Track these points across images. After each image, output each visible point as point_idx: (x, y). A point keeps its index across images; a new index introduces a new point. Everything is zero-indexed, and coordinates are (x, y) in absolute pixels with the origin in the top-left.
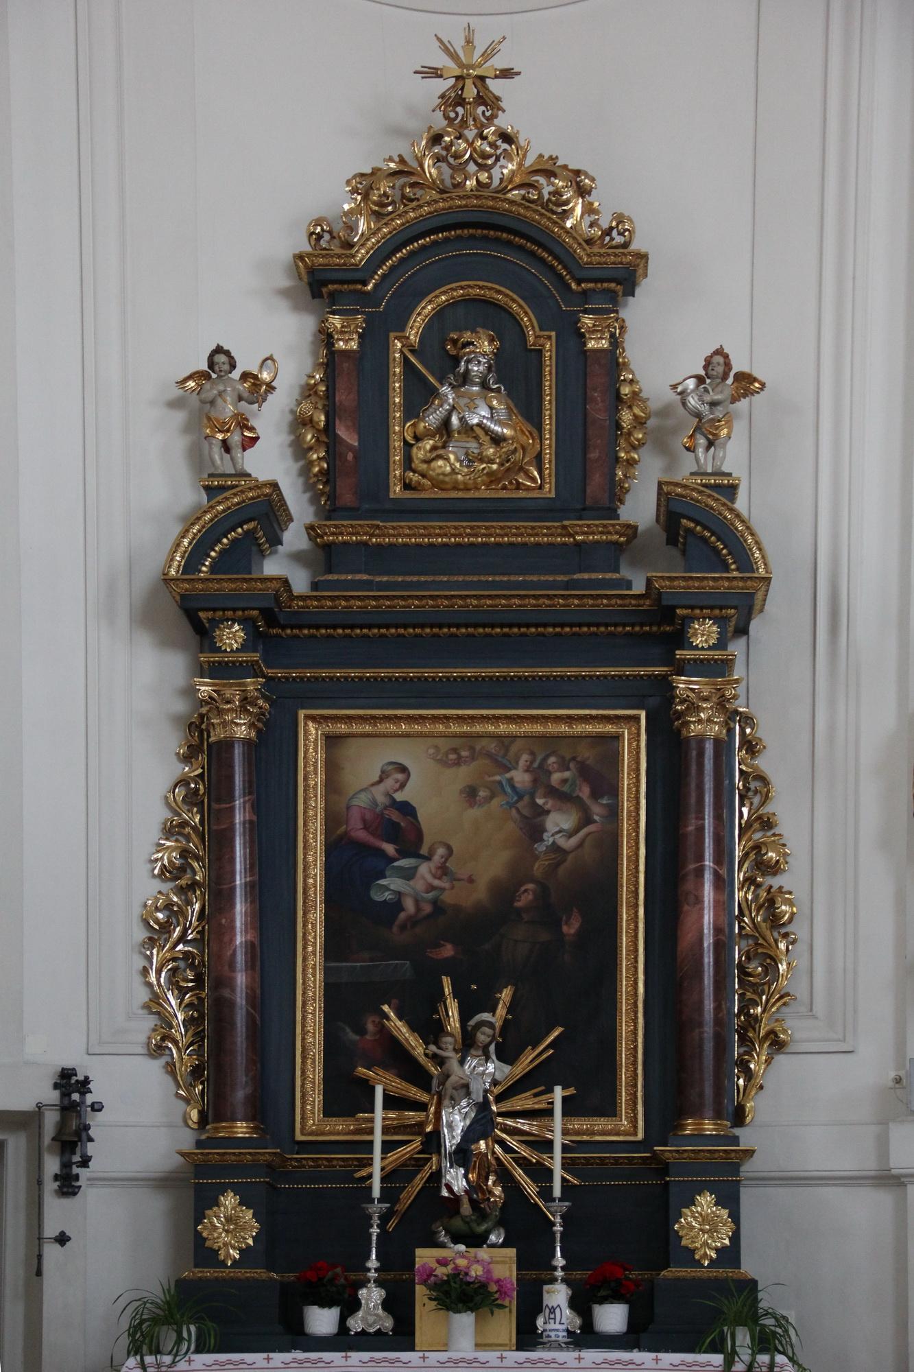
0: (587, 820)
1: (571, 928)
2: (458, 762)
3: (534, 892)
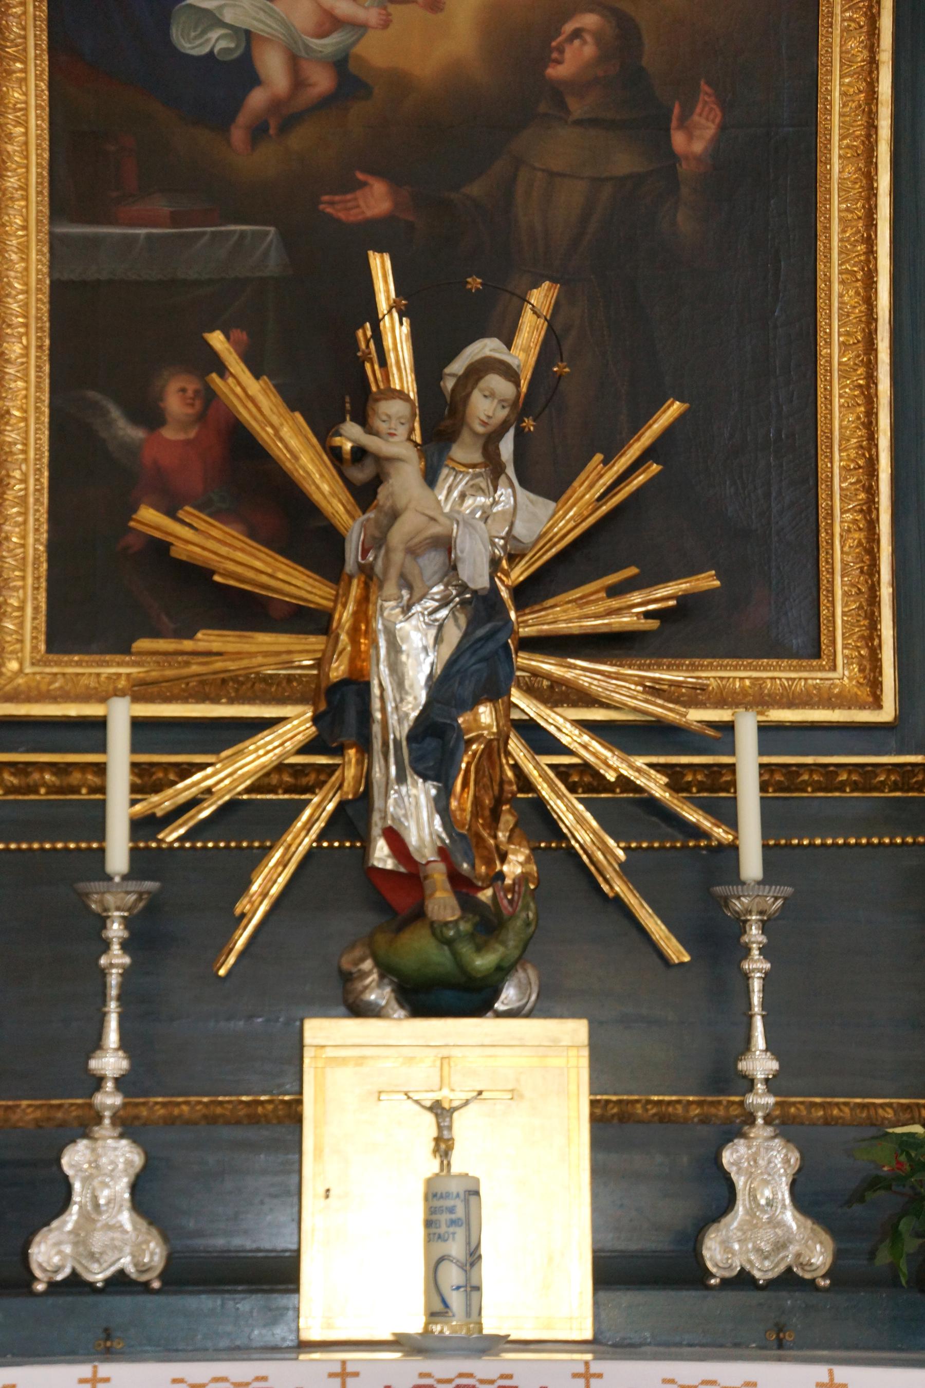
3: (599, 38)
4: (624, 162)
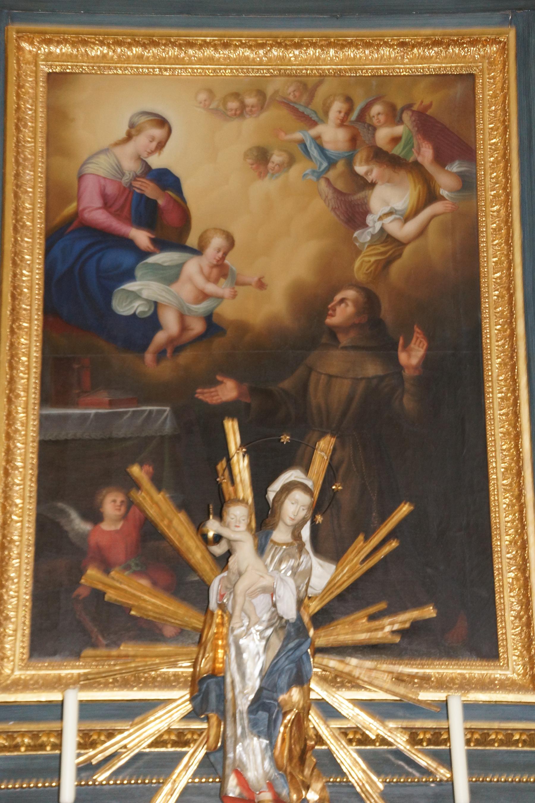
0: (430, 196)
1: (412, 355)
2: (242, 112)
3: (356, 303)
4: (372, 369)
